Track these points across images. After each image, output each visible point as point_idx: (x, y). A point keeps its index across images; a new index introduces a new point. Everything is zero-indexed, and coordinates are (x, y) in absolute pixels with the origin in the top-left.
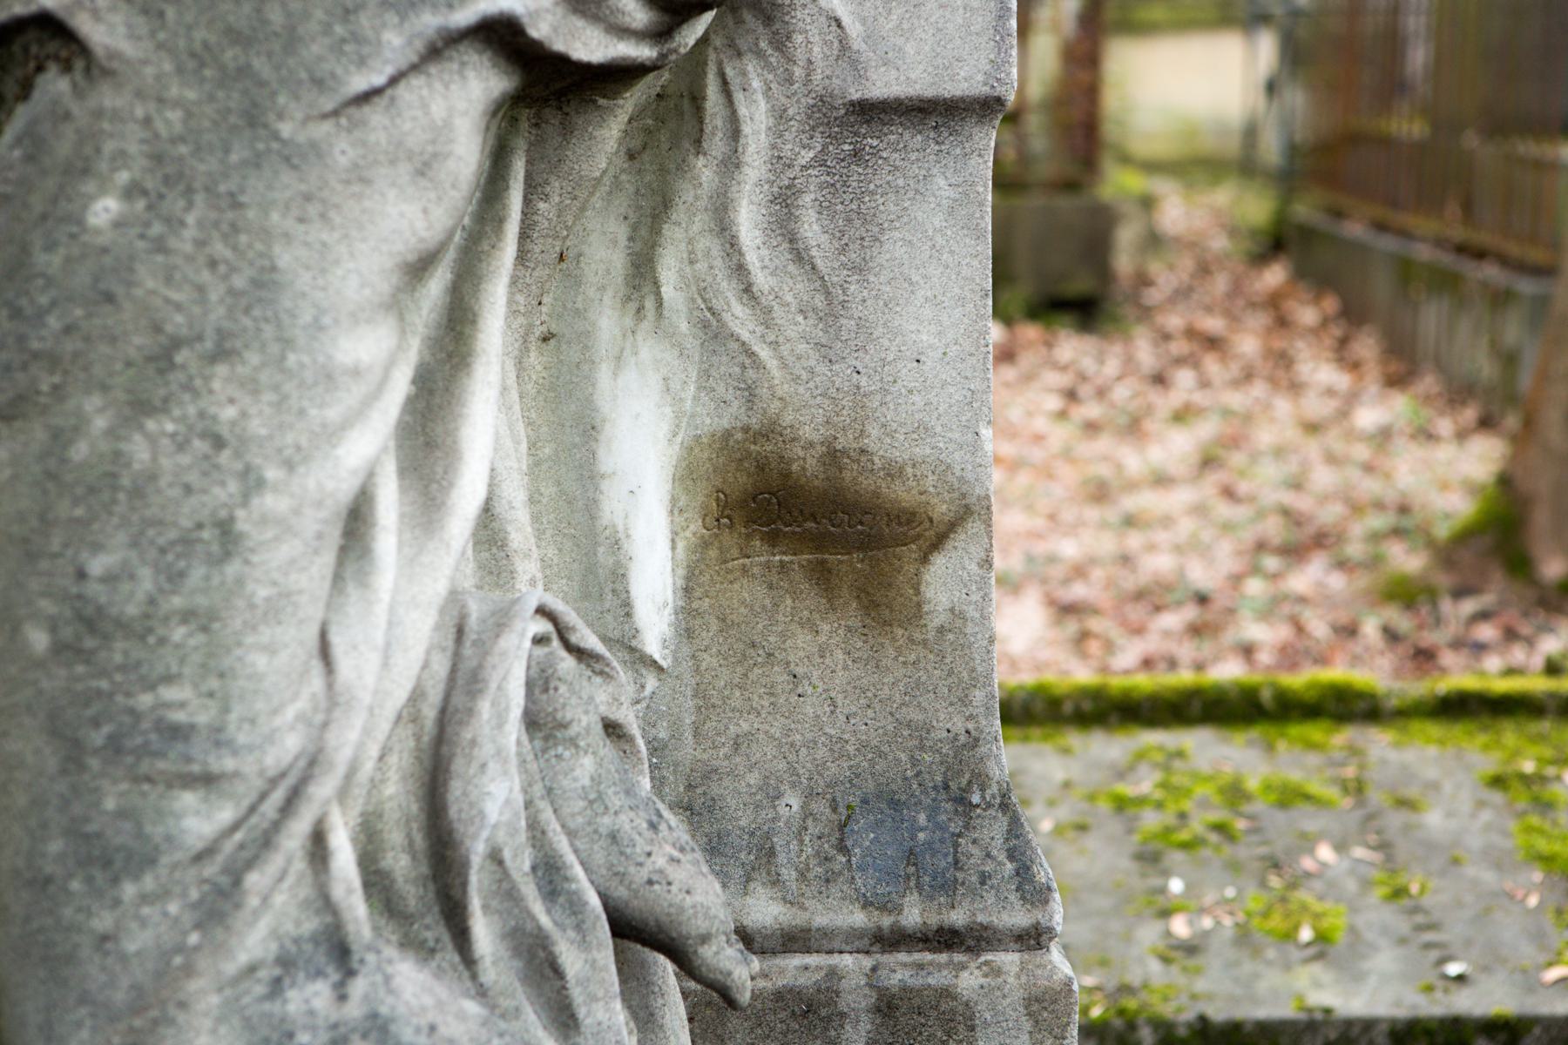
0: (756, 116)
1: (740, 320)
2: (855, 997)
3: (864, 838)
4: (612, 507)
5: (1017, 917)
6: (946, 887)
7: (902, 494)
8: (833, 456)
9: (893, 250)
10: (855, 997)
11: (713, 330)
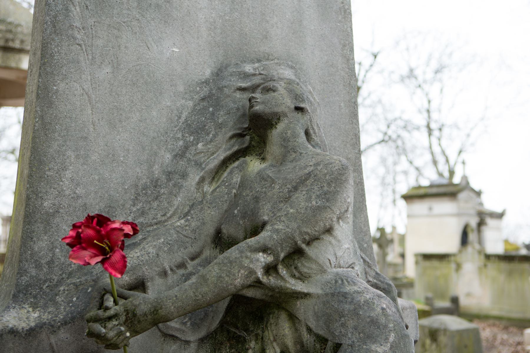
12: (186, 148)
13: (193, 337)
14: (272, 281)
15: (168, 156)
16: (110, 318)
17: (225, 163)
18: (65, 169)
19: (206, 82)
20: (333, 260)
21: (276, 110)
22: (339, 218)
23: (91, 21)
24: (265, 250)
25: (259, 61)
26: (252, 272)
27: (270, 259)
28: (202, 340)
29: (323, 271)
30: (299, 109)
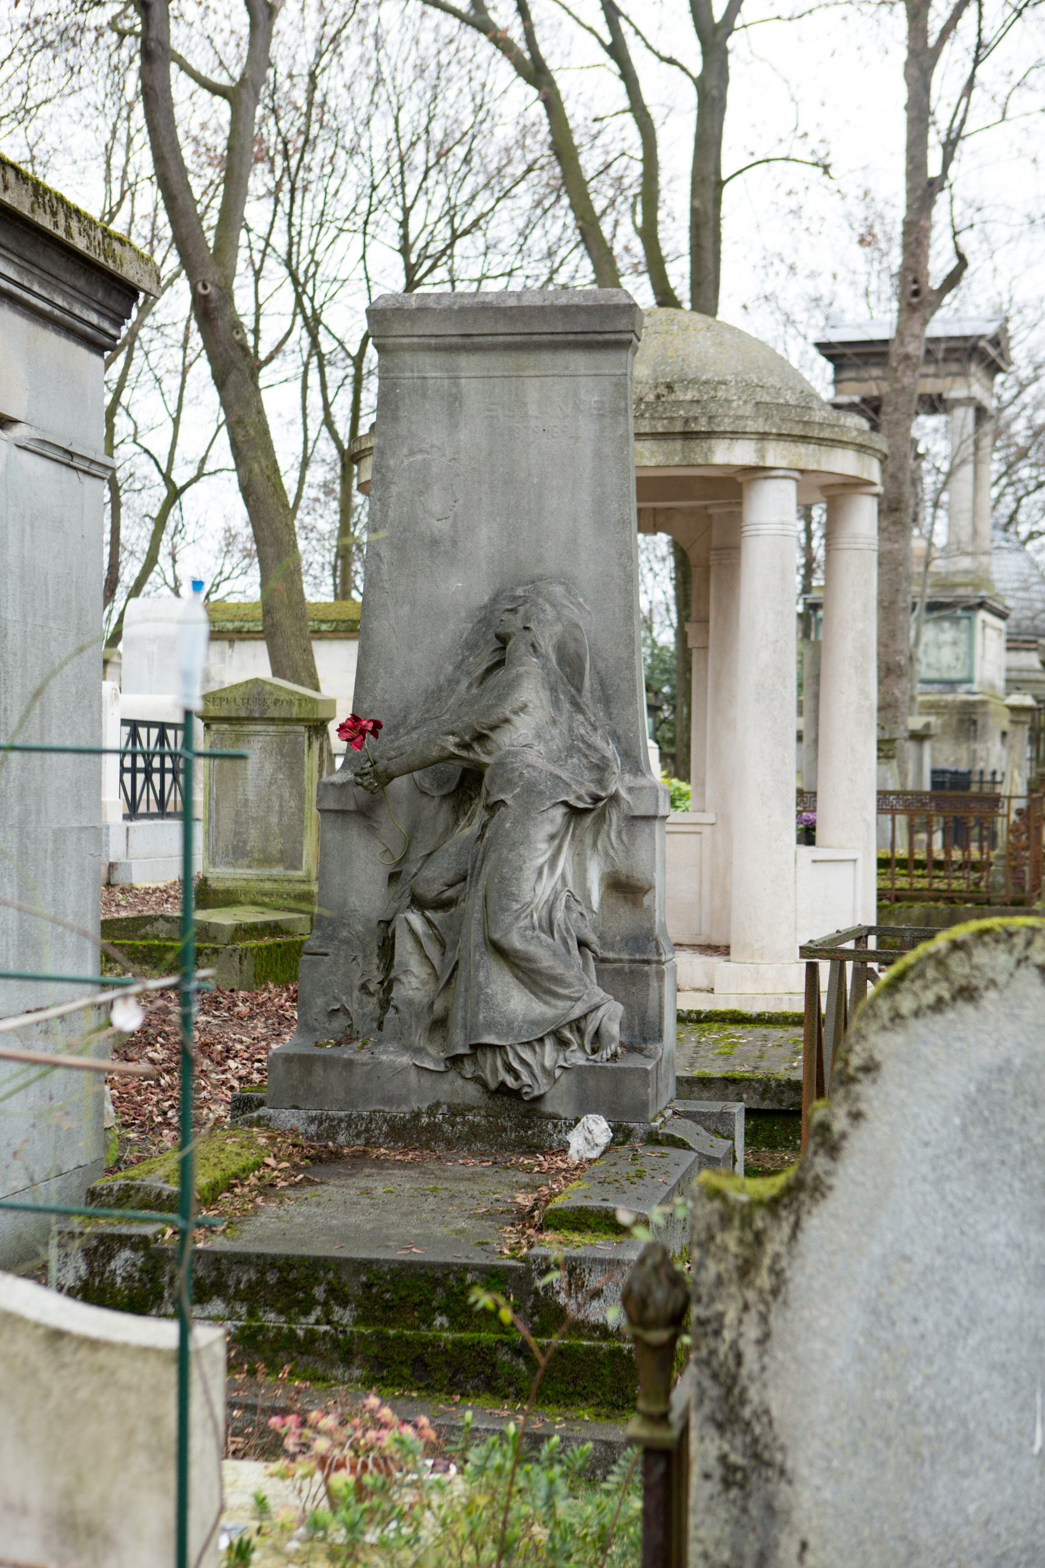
0: (614, 818)
1: (611, 852)
2: (627, 969)
3: (630, 944)
4: (589, 884)
5: (656, 958)
6: (644, 952)
7: (640, 884)
8: (628, 877)
9: (639, 841)
10: (627, 969)
11: (607, 854)
12: (463, 661)
13: (437, 794)
14: (471, 755)
15: (451, 668)
16: (366, 774)
17: (489, 671)
18: (377, 682)
19: (485, 607)
20: (507, 741)
21: (509, 630)
22: (515, 713)
23: (395, 574)
24: (453, 734)
25: (533, 582)
26: (443, 748)
27: (457, 740)
28: (444, 797)
29: (500, 749)
30: (526, 628)
